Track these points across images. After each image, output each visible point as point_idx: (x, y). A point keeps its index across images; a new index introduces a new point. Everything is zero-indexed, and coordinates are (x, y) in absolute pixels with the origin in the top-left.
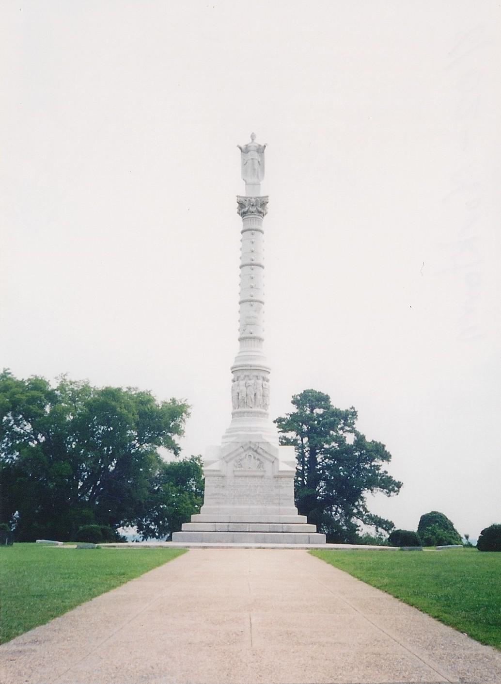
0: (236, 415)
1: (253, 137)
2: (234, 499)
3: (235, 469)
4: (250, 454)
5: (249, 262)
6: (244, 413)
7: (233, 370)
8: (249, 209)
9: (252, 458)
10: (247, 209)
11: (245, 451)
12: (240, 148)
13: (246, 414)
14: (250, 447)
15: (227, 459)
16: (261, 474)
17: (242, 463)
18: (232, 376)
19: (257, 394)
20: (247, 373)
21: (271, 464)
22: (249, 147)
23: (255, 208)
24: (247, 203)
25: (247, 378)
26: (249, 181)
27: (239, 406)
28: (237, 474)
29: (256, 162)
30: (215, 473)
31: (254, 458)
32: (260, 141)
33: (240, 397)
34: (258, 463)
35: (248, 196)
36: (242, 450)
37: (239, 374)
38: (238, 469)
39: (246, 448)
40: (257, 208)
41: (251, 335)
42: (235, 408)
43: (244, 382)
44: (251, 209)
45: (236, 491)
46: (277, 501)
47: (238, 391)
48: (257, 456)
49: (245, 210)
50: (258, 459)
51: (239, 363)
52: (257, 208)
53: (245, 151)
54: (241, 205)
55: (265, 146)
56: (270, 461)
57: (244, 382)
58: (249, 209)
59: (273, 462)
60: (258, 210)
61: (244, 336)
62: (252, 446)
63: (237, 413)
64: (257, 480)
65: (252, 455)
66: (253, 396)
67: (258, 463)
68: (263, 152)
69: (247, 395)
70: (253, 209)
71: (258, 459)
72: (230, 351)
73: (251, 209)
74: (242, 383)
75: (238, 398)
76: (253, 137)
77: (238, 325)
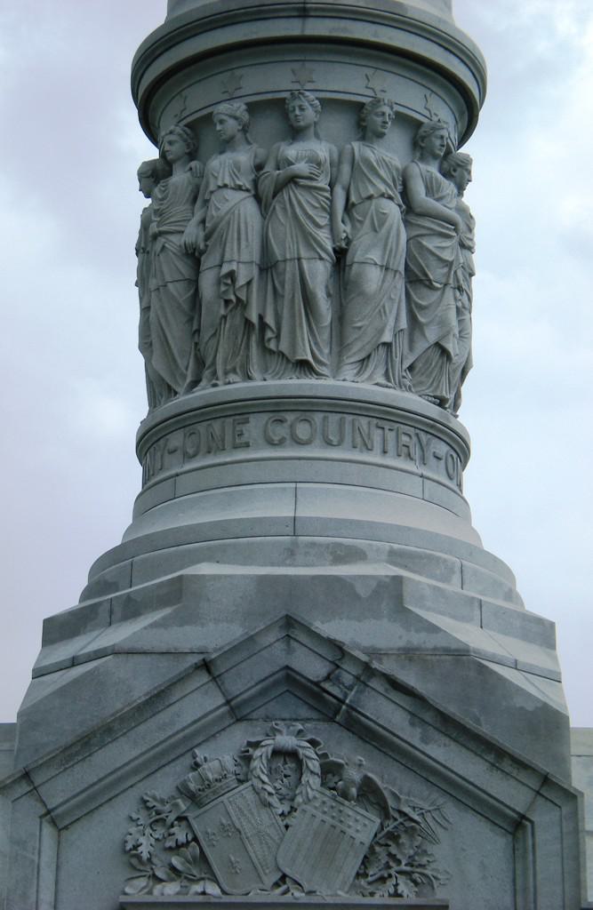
0: (176, 440)
4: (286, 740)
11: (237, 712)
14: (290, 679)
19: (357, 254)
27: (200, 363)
31: (330, 770)
34: (363, 826)
36: (199, 702)
39: (242, 682)
42: (158, 388)
43: (243, 157)
47: (192, 233)
50: (369, 793)
57: (243, 157)
59: (517, 826)
62: (312, 667)
67: (363, 826)
69: (268, 266)
71: (369, 793)
75: (196, 300)
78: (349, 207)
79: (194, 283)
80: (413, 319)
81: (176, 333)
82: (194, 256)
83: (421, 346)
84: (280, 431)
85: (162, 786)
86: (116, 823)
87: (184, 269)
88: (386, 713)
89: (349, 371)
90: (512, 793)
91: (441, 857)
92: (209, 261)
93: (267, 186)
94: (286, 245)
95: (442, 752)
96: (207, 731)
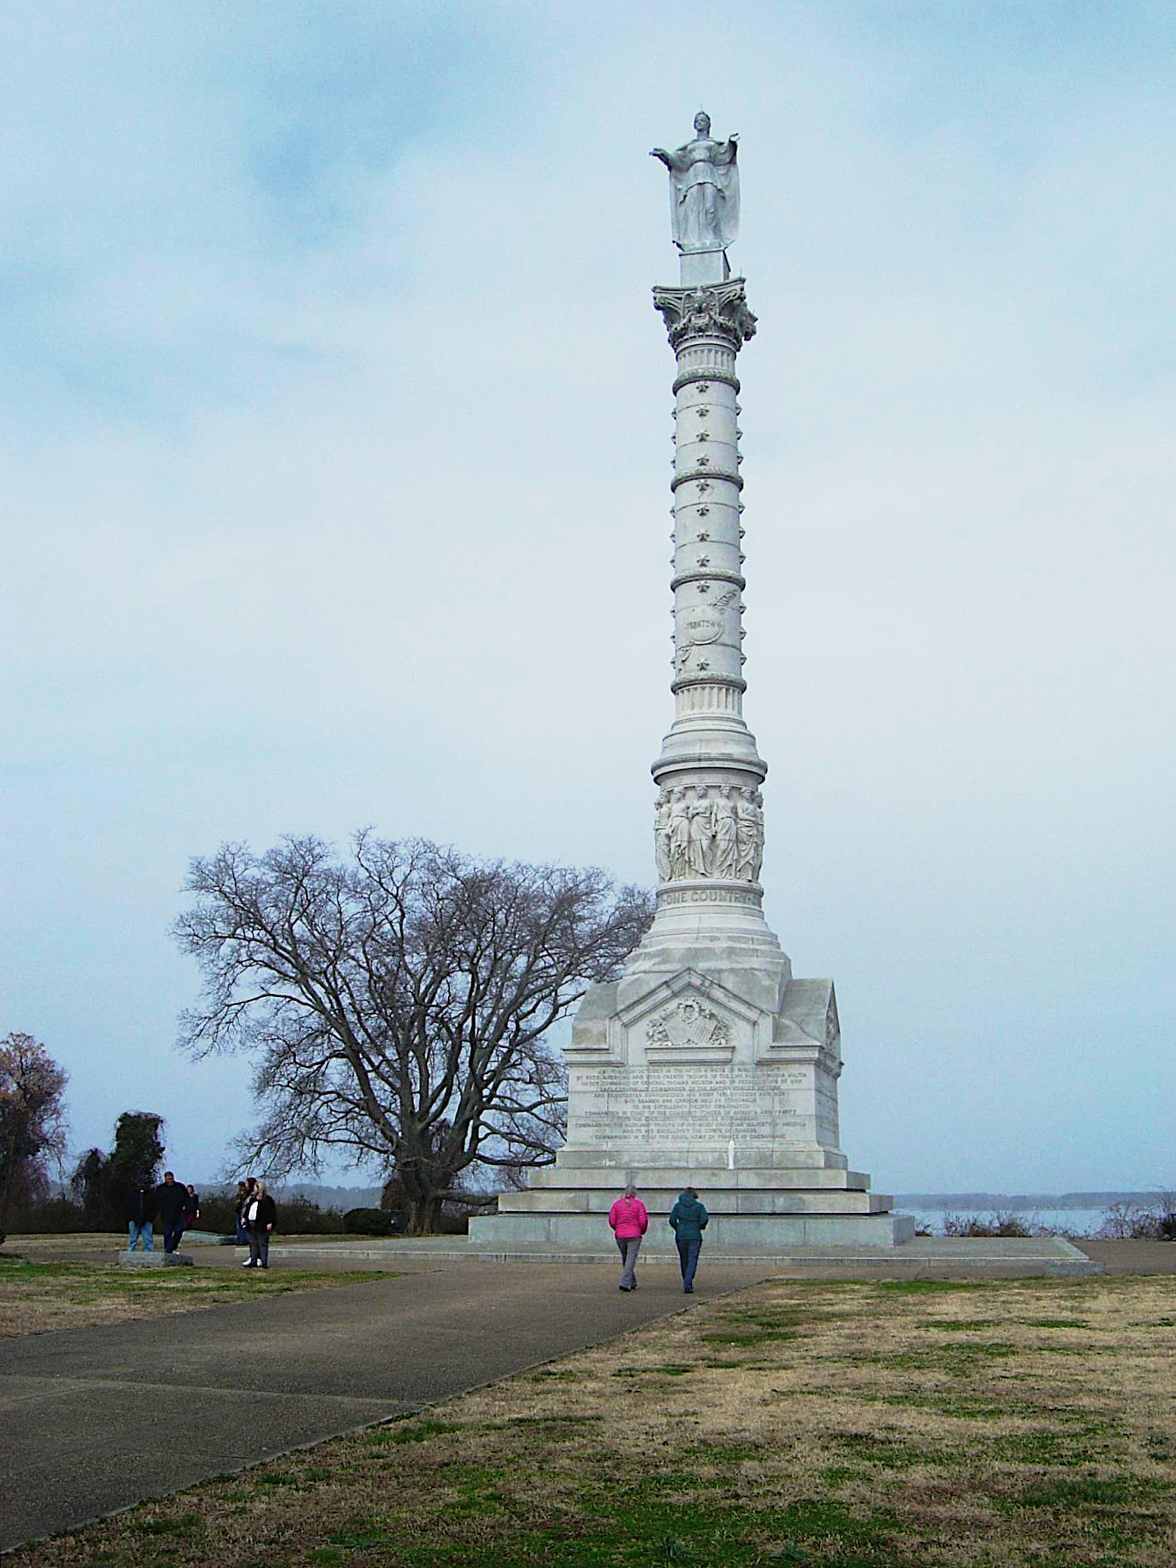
0: (665, 897)
1: (703, 126)
2: (648, 1125)
3: (648, 1044)
4: (689, 1003)
5: (690, 466)
6: (684, 889)
8: (690, 320)
9: (696, 1014)
10: (685, 321)
11: (675, 995)
12: (663, 157)
14: (690, 985)
15: (626, 1018)
16: (726, 1055)
17: (667, 1026)
18: (656, 792)
20: (688, 780)
21: (745, 1027)
22: (693, 150)
23: (707, 317)
24: (680, 305)
25: (690, 793)
26: (693, 241)
28: (656, 1057)
29: (709, 190)
31: (701, 1010)
32: (720, 133)
33: (673, 846)
35: (687, 285)
37: (670, 783)
38: (656, 1045)
39: (676, 987)
40: (711, 318)
43: (682, 805)
44: (712, 321)
45: (652, 1105)
46: (766, 1130)
47: (668, 831)
48: (708, 1006)
49: (679, 326)
50: (712, 1016)
51: (671, 754)
52: (711, 318)
53: (675, 164)
54: (669, 312)
55: (733, 145)
56: (748, 1020)
57: (682, 805)
58: (690, 320)
59: (754, 1023)
61: (684, 676)
62: (698, 982)
63: (666, 891)
64: (709, 1074)
65: (696, 1006)
66: (705, 843)
68: (733, 161)
70: (702, 321)
72: (653, 720)
73: (712, 321)
74: (677, 807)
76: (703, 126)
77: (670, 651)
79: (668, 845)
80: (739, 855)
81: (665, 860)
82: (669, 837)
83: (742, 863)
84: (696, 897)
85: (655, 1016)
86: (644, 1026)
87: (666, 841)
88: (718, 994)
89: (717, 874)
90: (753, 1015)
91: (733, 1032)
92: (673, 840)
95: (734, 1004)
96: (666, 1000)
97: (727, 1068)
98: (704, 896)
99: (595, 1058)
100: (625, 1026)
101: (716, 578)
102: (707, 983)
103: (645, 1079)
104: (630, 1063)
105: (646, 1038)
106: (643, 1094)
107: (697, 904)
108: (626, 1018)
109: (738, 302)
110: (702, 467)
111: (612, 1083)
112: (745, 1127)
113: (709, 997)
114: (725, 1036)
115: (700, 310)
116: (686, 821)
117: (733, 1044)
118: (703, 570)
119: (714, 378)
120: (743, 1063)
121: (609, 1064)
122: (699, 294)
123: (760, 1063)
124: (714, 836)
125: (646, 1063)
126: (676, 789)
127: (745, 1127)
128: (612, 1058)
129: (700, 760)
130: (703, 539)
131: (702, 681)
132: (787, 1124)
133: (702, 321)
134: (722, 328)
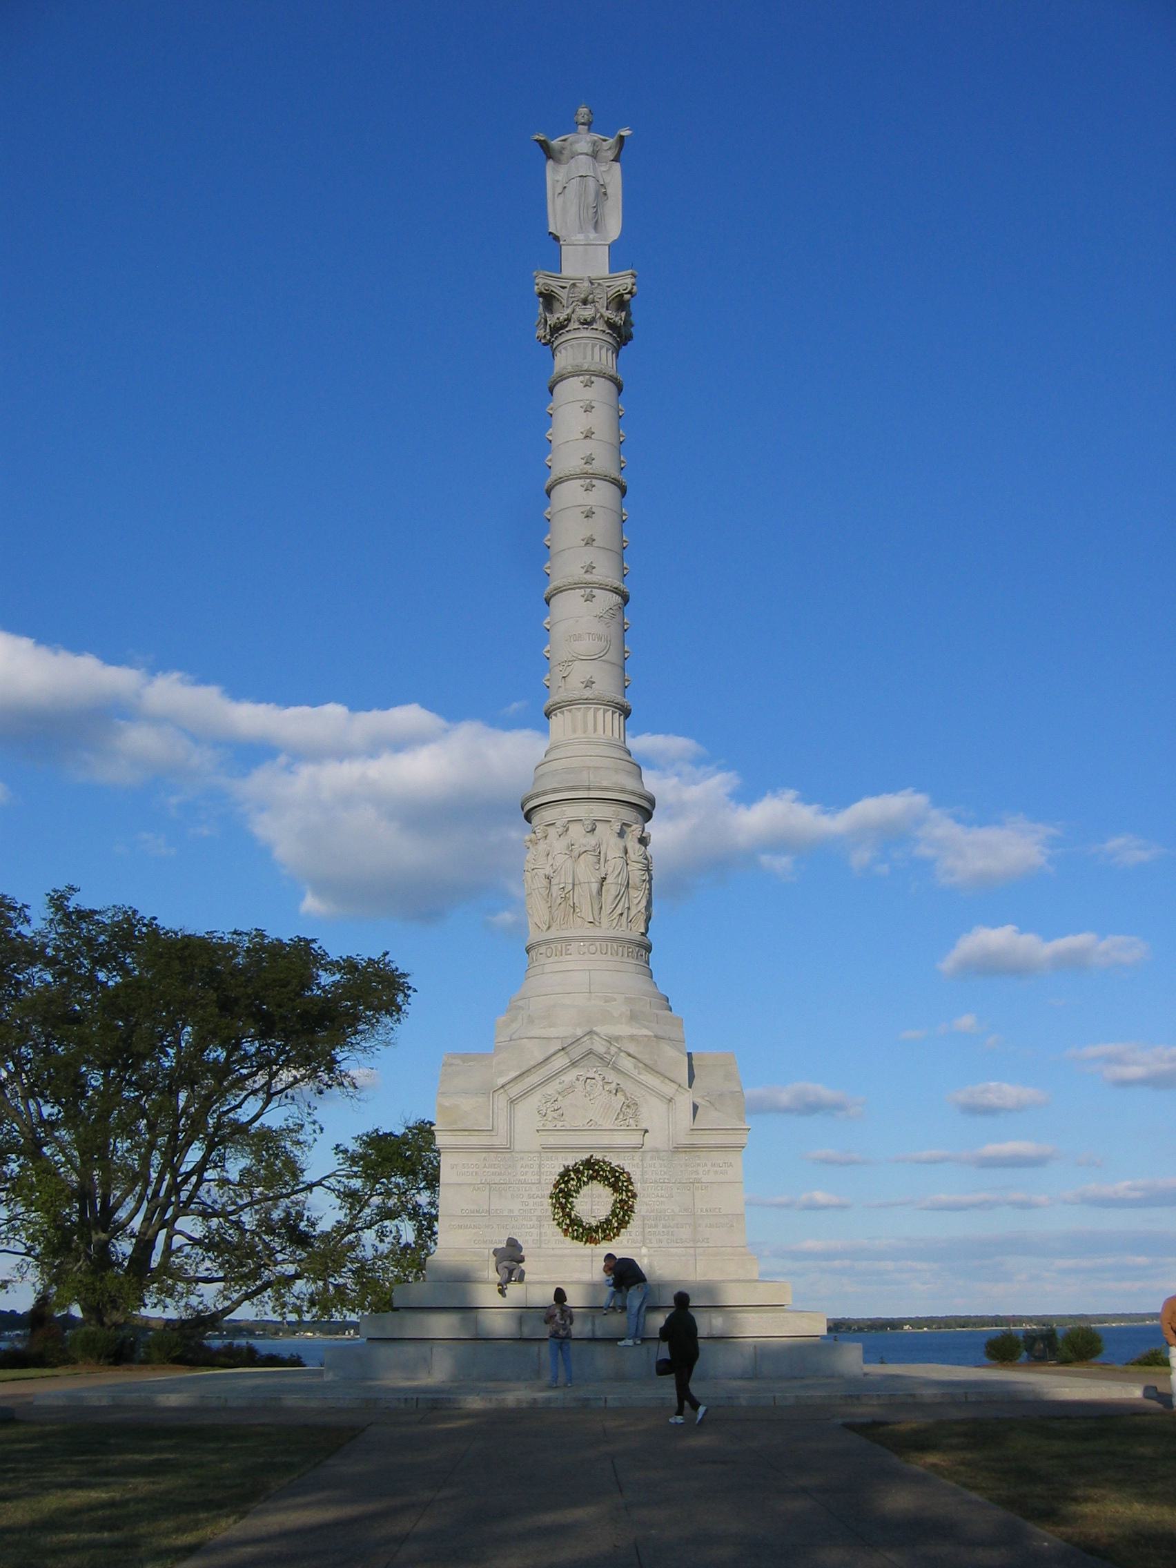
6: (569, 940)
7: (527, 807)
10: (569, 311)
11: (574, 1064)
13: (575, 945)
14: (590, 1052)
15: (515, 1090)
16: (635, 1139)
19: (609, 880)
20: (571, 811)
24: (563, 294)
28: (552, 1140)
29: (591, 183)
30: (474, 1140)
33: (555, 889)
39: (576, 1052)
40: (597, 311)
41: (587, 693)
43: (564, 842)
47: (548, 871)
48: (612, 1077)
52: (597, 311)
56: (661, 1096)
57: (564, 842)
60: (602, 316)
62: (600, 1047)
78: (606, 861)
85: (552, 1089)
86: (535, 1100)
87: (545, 882)
90: (669, 1089)
93: (576, 853)
94: (582, 877)
96: (562, 1071)
97: (637, 1156)
98: (593, 949)
99: (474, 1140)
100: (512, 1102)
101: (602, 587)
102: (613, 1050)
103: (536, 1169)
104: (517, 1148)
105: (538, 1117)
106: (534, 1187)
107: (585, 957)
108: (515, 1090)
109: (627, 297)
110: (588, 466)
111: (494, 1174)
112: (660, 1229)
113: (615, 1068)
114: (635, 1115)
115: (585, 302)
116: (569, 863)
117: (644, 1126)
118: (588, 577)
119: (601, 375)
120: (657, 1151)
121: (490, 1149)
122: (587, 284)
123: (677, 1149)
124: (604, 879)
125: (539, 1148)
126: (559, 823)
127: (660, 1229)
128: (496, 1141)
129: (589, 789)
130: (589, 542)
131: (587, 701)
132: (711, 1226)
133: (588, 313)
134: (611, 325)
